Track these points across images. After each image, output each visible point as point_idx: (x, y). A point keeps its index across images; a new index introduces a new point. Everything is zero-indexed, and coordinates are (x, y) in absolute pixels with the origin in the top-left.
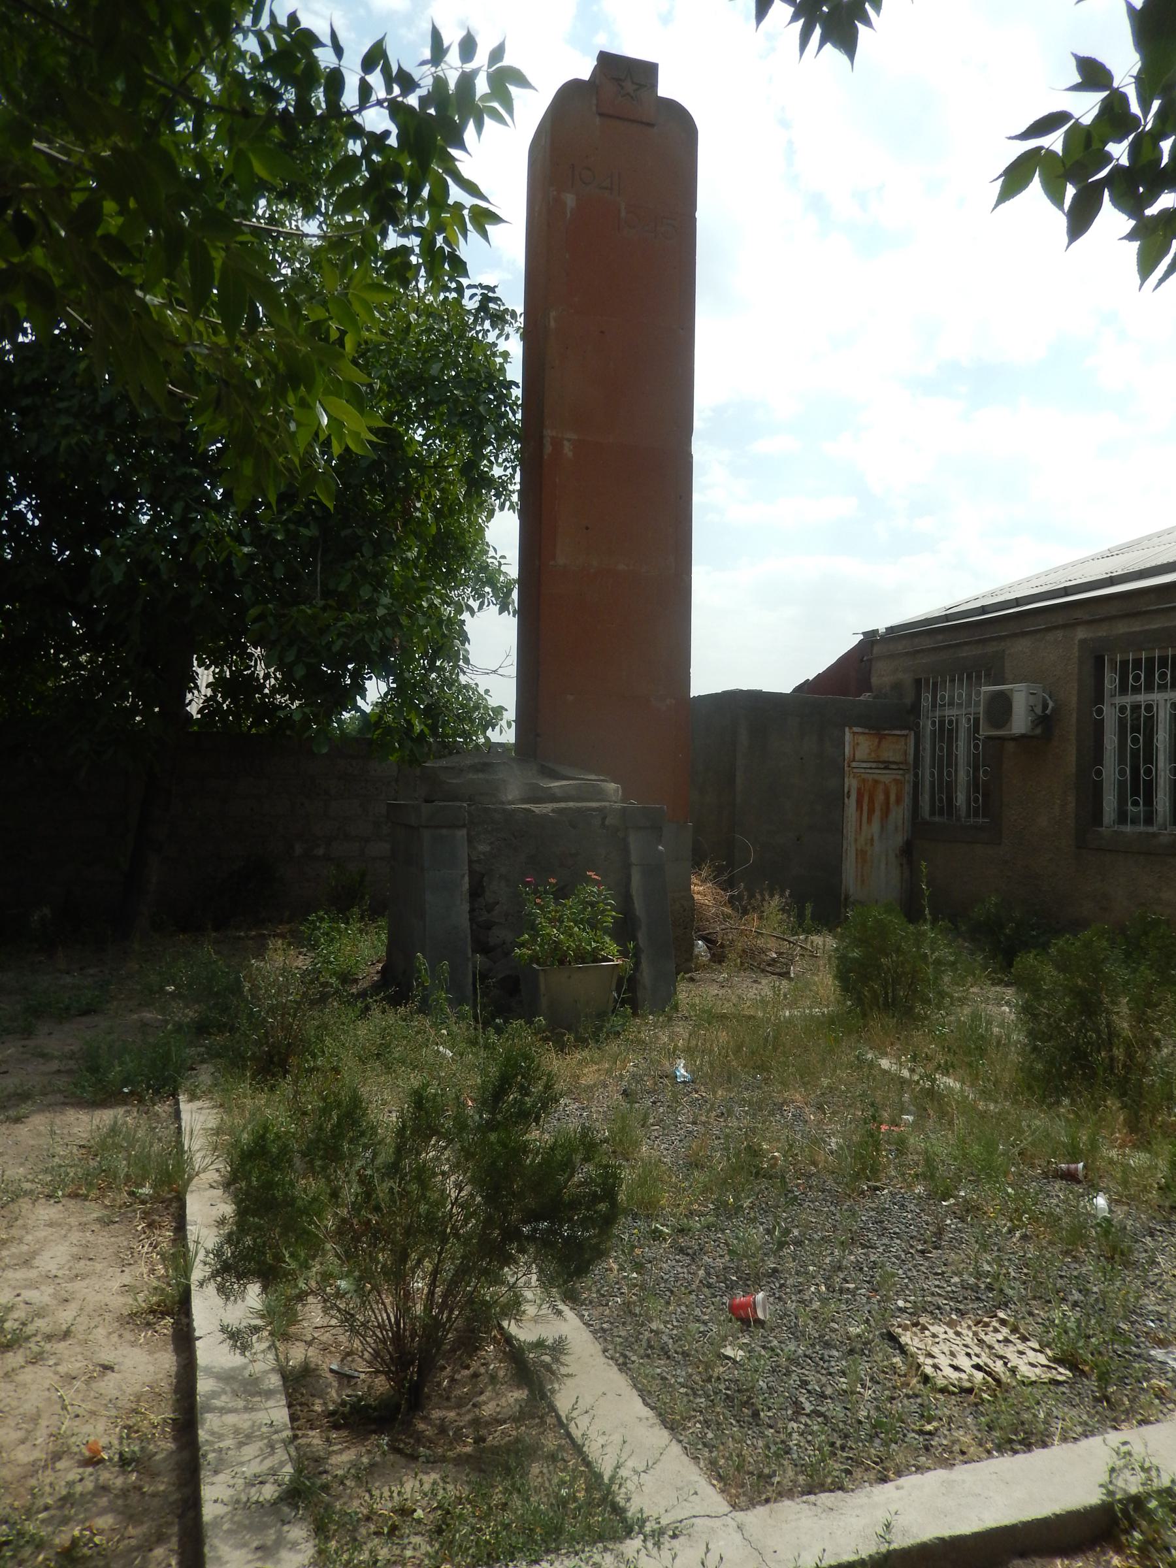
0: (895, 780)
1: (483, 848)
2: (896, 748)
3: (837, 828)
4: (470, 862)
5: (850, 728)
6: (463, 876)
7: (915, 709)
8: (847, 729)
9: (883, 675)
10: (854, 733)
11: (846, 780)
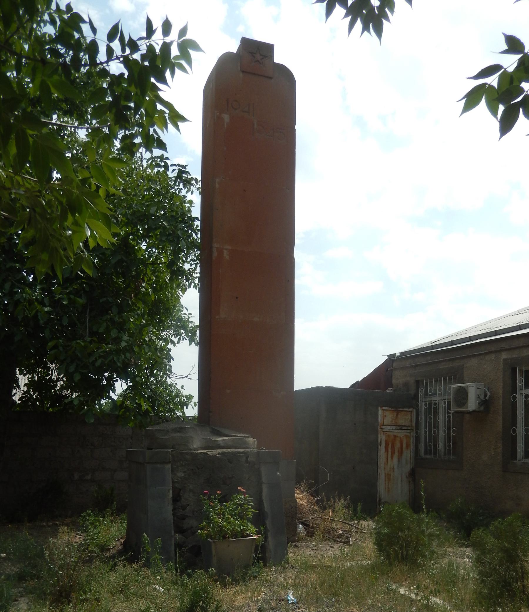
0: (405, 435)
3: (375, 463)
5: (381, 407)
7: (416, 397)
8: (379, 408)
10: (383, 410)
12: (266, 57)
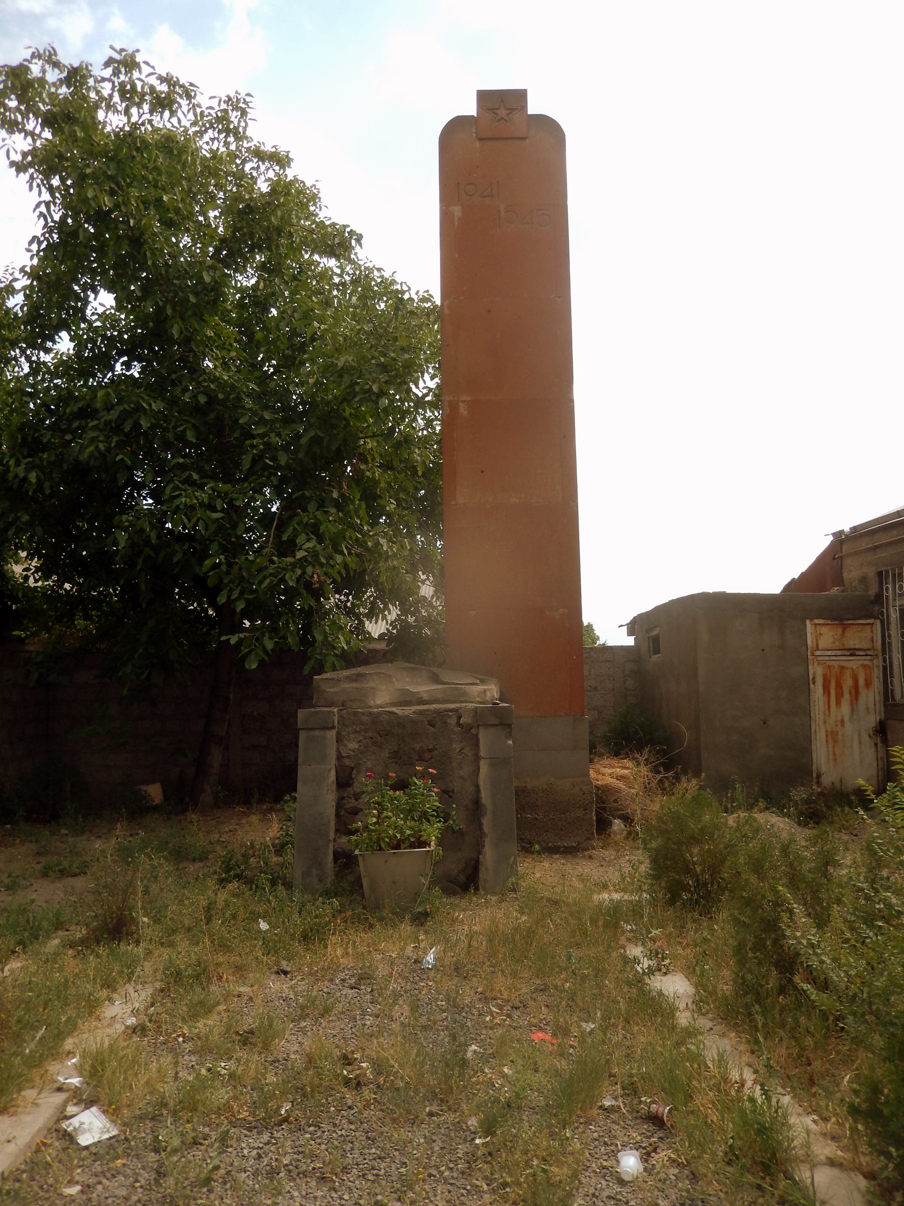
0: (862, 665)
1: (353, 745)
2: (862, 635)
3: (806, 712)
4: (339, 757)
5: (811, 620)
6: (330, 770)
7: (879, 599)
8: (808, 622)
9: (853, 572)
10: (816, 625)
11: (810, 667)
12: (513, 110)
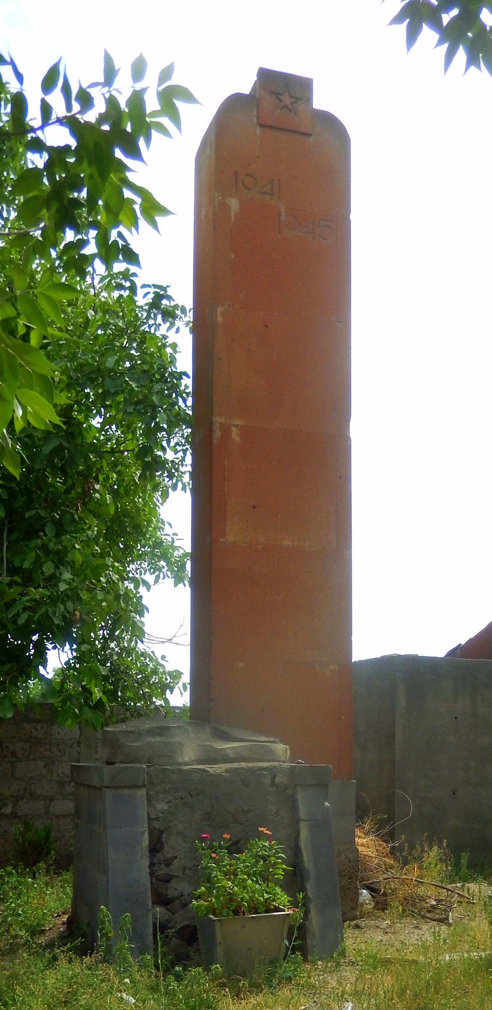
1: (162, 806)
4: (150, 819)
6: (143, 833)
12: (298, 99)
